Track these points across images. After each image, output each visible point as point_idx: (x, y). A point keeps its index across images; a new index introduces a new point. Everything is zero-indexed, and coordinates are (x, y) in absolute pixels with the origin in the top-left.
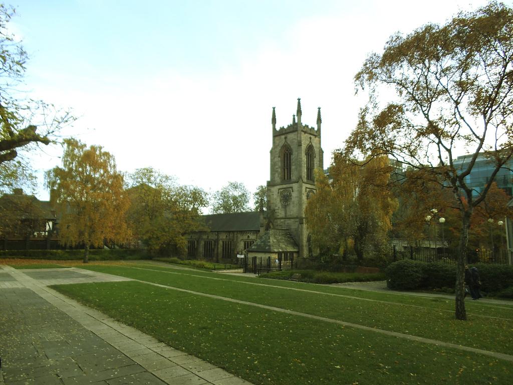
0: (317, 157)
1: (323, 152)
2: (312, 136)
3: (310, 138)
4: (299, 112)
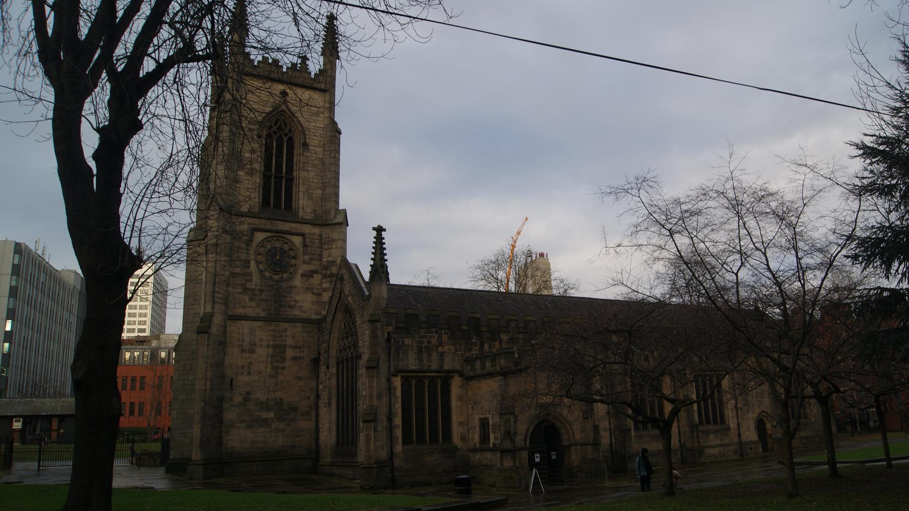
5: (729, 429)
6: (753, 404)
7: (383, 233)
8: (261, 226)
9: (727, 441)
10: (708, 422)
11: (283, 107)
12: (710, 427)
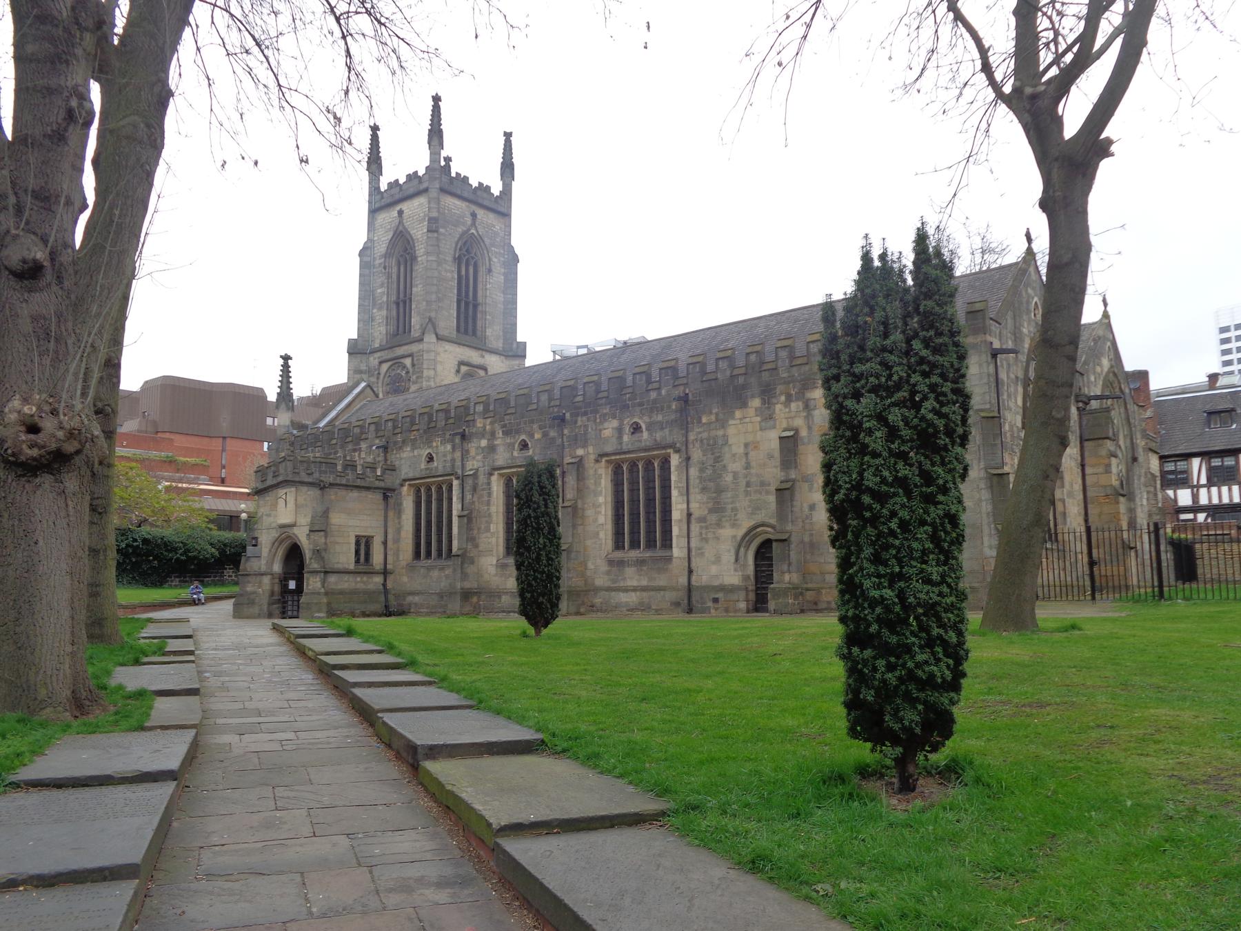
0: (498, 269)
1: (516, 259)
2: (481, 213)
3: (474, 215)
4: (436, 134)
5: (669, 559)
6: (734, 510)
7: (289, 361)
8: (384, 358)
9: (661, 581)
10: (635, 544)
11: (401, 228)
12: (634, 554)
